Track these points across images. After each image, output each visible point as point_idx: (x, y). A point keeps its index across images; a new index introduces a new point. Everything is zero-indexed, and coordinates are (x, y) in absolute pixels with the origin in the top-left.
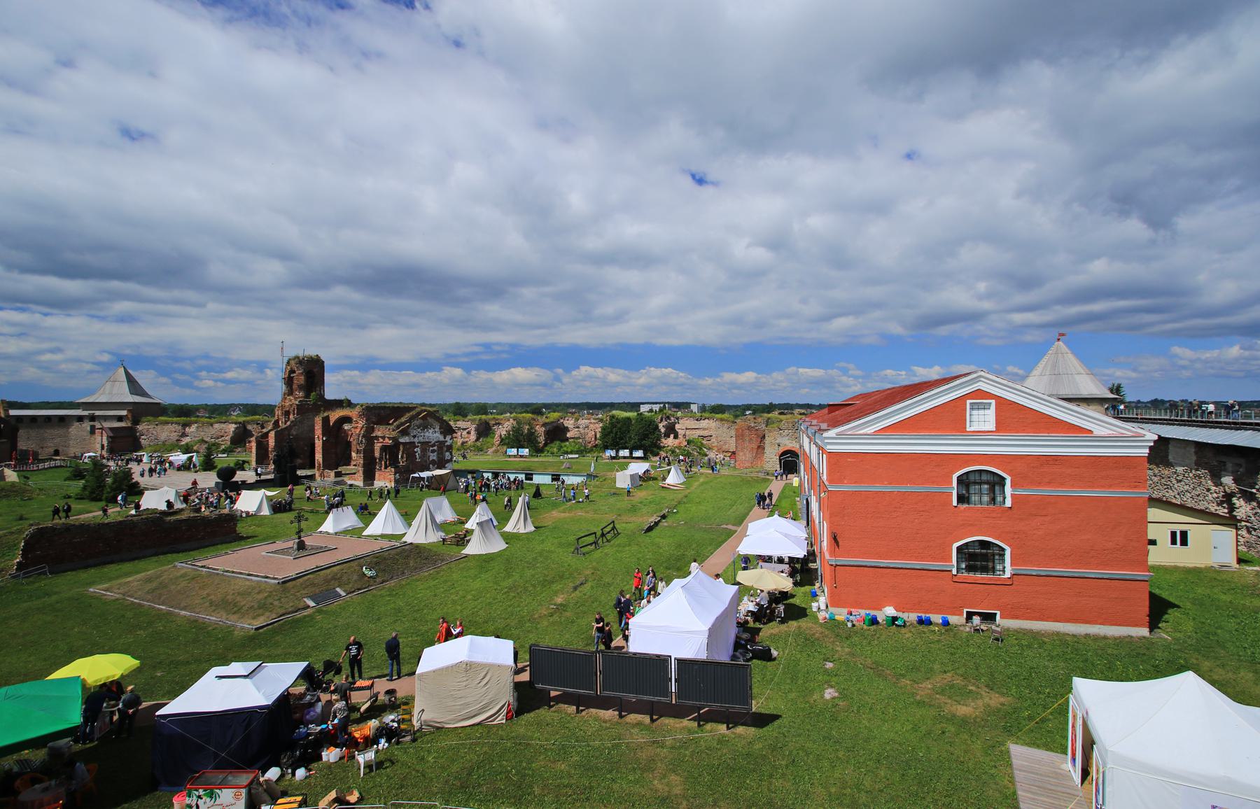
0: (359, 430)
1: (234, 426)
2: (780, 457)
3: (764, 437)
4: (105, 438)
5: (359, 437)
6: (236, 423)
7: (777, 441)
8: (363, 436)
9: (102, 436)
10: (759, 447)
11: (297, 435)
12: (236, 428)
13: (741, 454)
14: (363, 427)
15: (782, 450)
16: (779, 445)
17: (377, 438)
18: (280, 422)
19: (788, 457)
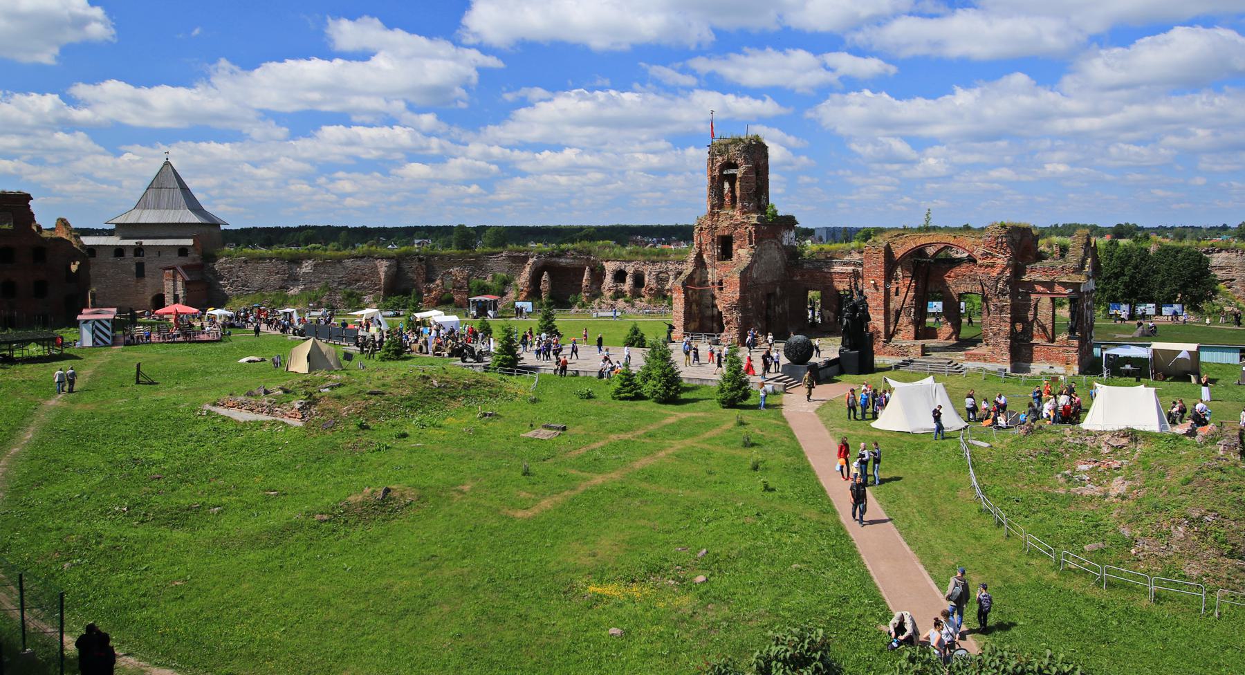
0: (998, 270)
1: (385, 263)
4: (179, 284)
5: (997, 282)
6: (388, 258)
8: (1007, 282)
9: (175, 281)
11: (757, 278)
12: (389, 267)
14: (1008, 266)
17: (1031, 284)
18: (705, 256)
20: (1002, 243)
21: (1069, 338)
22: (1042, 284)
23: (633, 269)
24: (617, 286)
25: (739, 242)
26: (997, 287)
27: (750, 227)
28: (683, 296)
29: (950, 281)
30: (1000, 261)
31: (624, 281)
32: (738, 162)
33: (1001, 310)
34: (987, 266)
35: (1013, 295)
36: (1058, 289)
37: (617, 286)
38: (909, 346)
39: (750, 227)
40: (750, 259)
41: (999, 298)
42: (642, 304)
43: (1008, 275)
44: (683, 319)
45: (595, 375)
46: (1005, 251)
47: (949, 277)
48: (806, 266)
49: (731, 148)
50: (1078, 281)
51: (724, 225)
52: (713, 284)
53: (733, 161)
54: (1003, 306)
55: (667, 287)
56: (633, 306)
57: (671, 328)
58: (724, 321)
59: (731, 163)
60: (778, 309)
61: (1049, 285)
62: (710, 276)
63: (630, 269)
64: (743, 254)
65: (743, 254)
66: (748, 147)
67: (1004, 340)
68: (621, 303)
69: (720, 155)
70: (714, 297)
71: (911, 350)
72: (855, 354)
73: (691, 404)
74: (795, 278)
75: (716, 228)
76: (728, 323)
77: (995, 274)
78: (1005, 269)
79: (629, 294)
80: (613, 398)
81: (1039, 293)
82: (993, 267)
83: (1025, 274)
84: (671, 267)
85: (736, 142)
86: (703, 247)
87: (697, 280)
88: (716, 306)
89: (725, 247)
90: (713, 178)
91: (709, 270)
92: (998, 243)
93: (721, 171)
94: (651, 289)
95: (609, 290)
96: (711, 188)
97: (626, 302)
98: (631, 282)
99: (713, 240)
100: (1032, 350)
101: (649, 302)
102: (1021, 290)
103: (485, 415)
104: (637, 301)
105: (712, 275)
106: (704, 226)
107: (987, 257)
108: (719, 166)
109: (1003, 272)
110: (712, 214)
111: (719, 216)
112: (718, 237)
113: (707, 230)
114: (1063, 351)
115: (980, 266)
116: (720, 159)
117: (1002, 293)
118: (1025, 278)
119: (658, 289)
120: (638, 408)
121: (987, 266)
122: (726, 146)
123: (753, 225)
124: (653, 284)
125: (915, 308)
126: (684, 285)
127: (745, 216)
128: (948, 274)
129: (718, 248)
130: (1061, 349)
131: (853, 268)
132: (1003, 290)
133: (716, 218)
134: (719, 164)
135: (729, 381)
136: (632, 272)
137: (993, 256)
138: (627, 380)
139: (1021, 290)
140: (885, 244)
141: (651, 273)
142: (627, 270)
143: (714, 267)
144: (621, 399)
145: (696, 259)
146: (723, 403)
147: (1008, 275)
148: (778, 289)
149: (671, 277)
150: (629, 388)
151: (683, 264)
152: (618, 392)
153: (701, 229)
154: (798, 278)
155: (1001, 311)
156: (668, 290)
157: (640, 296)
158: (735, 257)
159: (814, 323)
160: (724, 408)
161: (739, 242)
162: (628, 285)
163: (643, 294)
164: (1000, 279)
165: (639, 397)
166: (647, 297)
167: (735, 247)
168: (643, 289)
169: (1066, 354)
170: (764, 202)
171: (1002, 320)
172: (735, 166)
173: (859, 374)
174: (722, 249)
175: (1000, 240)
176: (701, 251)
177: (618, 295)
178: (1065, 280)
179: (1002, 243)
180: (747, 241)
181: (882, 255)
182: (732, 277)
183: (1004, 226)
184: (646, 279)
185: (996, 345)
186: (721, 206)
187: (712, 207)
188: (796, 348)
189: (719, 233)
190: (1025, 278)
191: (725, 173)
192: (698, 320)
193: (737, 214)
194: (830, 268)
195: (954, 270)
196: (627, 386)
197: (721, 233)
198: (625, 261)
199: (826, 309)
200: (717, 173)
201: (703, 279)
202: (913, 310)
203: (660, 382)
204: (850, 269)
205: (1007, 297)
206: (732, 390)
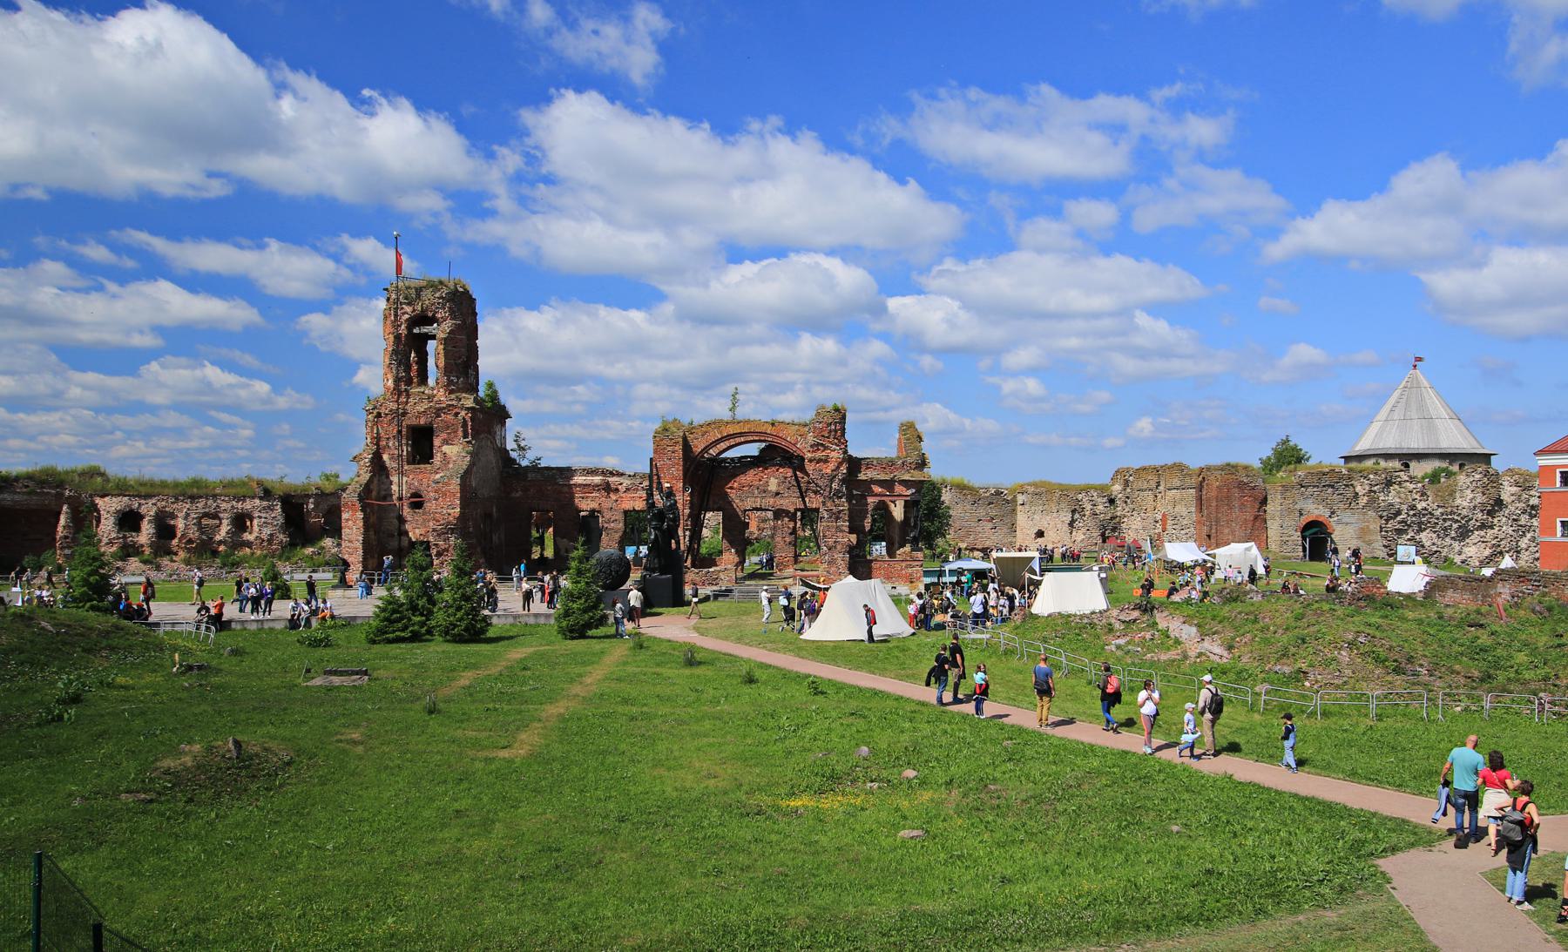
0: (832, 466)
2: (1301, 533)
3: (1264, 501)
5: (832, 481)
7: (1298, 507)
8: (843, 481)
10: (1256, 518)
13: (1226, 531)
15: (1304, 521)
16: (1301, 514)
17: (869, 483)
18: (385, 457)
19: (1315, 533)
20: (836, 431)
21: (912, 550)
22: (881, 483)
23: (155, 509)
24: (125, 537)
25: (444, 435)
26: (831, 487)
27: (463, 413)
28: (360, 515)
29: (732, 494)
30: (833, 454)
31: (137, 529)
32: (439, 316)
33: (836, 516)
34: (819, 461)
35: (850, 498)
36: (899, 489)
37: (125, 537)
38: (719, 571)
39: (463, 413)
40: (468, 459)
41: (834, 502)
42: (175, 565)
43: (845, 471)
44: (360, 552)
45: (279, 626)
46: (840, 441)
47: (731, 488)
48: (530, 476)
49: (427, 295)
50: (923, 479)
51: (417, 409)
52: (400, 499)
53: (430, 314)
54: (840, 512)
55: (218, 538)
56: (158, 568)
57: (346, 564)
58: (434, 552)
59: (427, 316)
60: (495, 538)
61: (888, 485)
62: (394, 488)
63: (149, 509)
64: (453, 452)
65: (453, 452)
66: (454, 295)
67: (841, 555)
68: (134, 563)
69: (409, 304)
70: (402, 520)
71: (722, 576)
72: (668, 578)
73: (506, 642)
74: (513, 495)
75: (404, 414)
76: (439, 554)
77: (829, 471)
78: (840, 464)
79: (147, 551)
80: (374, 642)
81: (876, 495)
82: (826, 461)
83: (860, 472)
84: (224, 506)
85: (434, 286)
86: (383, 443)
87: (374, 494)
88: (406, 533)
89: (421, 444)
90: (398, 337)
91: (395, 479)
92: (830, 431)
93: (410, 328)
94: (190, 541)
95: (111, 543)
96: (395, 352)
97: (145, 562)
98: (152, 531)
99: (400, 432)
100: (870, 568)
101: (187, 562)
102: (855, 492)
103: (190, 668)
104: (165, 561)
105: (399, 485)
106: (383, 411)
107: (818, 449)
108: (407, 320)
109: (838, 467)
110: (397, 391)
111: (408, 396)
112: (408, 426)
113: (389, 417)
114: (906, 567)
115: (810, 461)
116: (408, 309)
117: (838, 494)
118: (862, 477)
119: (202, 540)
120: (431, 650)
121: (819, 461)
122: (419, 290)
123: (468, 409)
124: (193, 533)
125: (690, 530)
126: (361, 499)
127: (453, 396)
128: (730, 485)
129: (407, 445)
130: (904, 564)
131: (601, 477)
132: (838, 491)
133: (403, 399)
134: (407, 316)
135: (579, 598)
136: (152, 513)
137: (826, 448)
138: (394, 611)
139: (855, 492)
140: (681, 434)
141: (187, 515)
142: (143, 510)
143: (402, 473)
144: (390, 641)
145: (372, 461)
146: (571, 631)
147: (845, 471)
148: (494, 510)
149: (225, 522)
150: (400, 625)
151: (244, 501)
152: (381, 631)
153: (379, 415)
154: (519, 494)
155: (837, 518)
156: (220, 543)
157: (169, 552)
158: (437, 459)
159: (542, 558)
160: (573, 638)
161: (444, 435)
162: (146, 533)
163: (175, 549)
164: (835, 477)
165: (415, 638)
166: (182, 554)
167: (437, 442)
168: (175, 542)
169: (910, 570)
170: (472, 379)
171: (839, 529)
172: (431, 321)
173: (674, 607)
174: (412, 446)
175: (833, 427)
176: (378, 448)
177: (128, 551)
178: (907, 477)
179: (836, 431)
180: (460, 433)
181: (679, 448)
182: (447, 484)
183: (837, 410)
184: (180, 524)
185: (832, 562)
186: (409, 382)
187: (397, 380)
188: (610, 566)
189: (410, 420)
190: (862, 477)
191: (416, 331)
192: (376, 556)
193: (441, 395)
194: (570, 478)
195: (738, 479)
196: (399, 620)
197: (414, 422)
198: (140, 496)
199: (563, 538)
200: (403, 330)
201: (383, 493)
202: (688, 533)
203: (459, 608)
204: (597, 479)
205: (843, 500)
206: (585, 611)
